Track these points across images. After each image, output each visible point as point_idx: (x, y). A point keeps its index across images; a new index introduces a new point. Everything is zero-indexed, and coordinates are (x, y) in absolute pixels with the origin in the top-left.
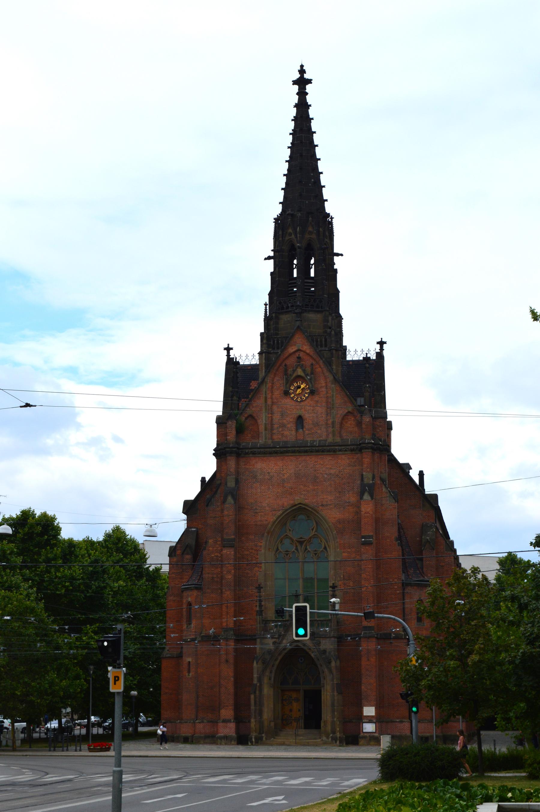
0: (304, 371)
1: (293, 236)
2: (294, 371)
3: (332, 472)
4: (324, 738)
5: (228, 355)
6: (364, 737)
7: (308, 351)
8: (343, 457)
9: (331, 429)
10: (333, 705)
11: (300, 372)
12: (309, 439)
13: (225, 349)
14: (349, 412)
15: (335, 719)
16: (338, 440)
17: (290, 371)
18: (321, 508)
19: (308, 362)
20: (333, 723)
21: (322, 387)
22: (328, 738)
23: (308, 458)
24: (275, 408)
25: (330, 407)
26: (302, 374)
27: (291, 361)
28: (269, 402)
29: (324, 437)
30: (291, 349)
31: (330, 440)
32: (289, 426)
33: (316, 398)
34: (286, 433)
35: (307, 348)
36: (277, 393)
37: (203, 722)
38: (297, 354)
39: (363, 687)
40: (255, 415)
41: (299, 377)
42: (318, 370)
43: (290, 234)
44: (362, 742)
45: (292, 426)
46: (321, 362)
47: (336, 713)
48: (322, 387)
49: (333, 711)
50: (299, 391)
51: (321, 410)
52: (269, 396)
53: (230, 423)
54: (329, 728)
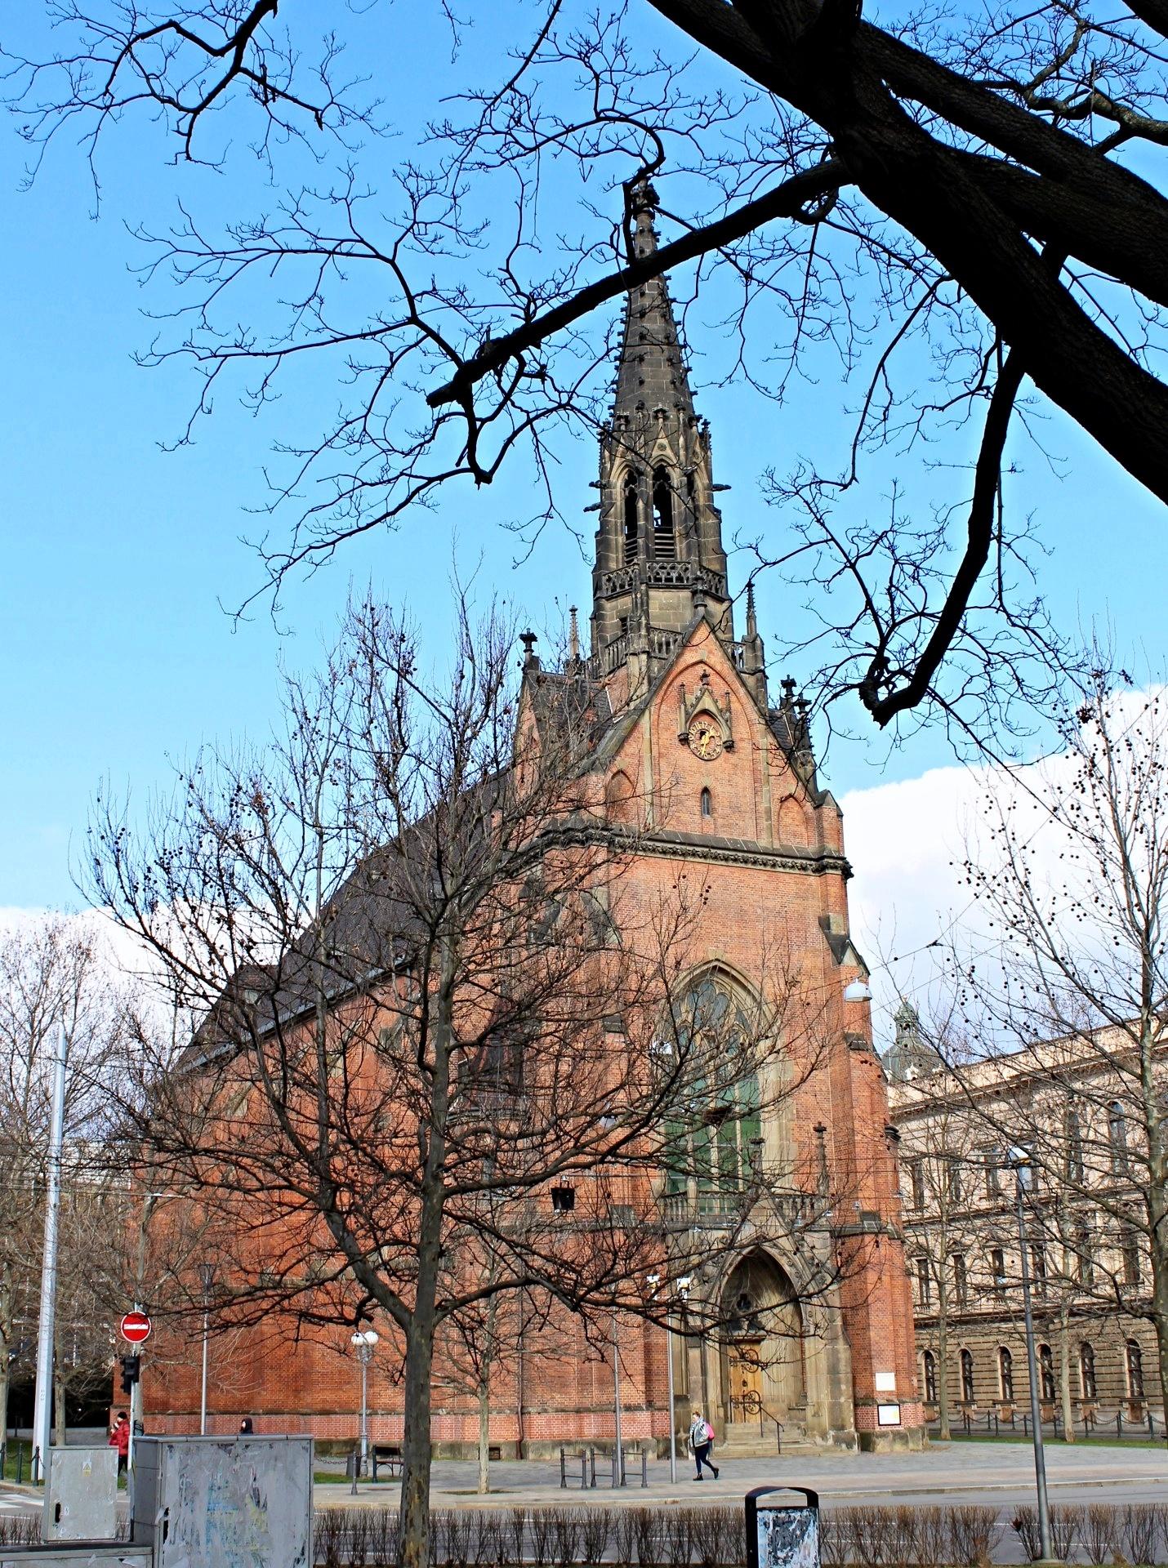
0: (716, 702)
1: (669, 452)
2: (698, 699)
3: (769, 904)
4: (819, 1440)
5: (529, 650)
6: (883, 1435)
7: (718, 668)
8: (786, 877)
9: (764, 823)
10: (833, 1370)
11: (707, 703)
12: (725, 836)
13: (523, 637)
14: (791, 796)
15: (842, 1400)
16: (777, 845)
17: (690, 699)
18: (754, 972)
19: (718, 686)
20: (835, 1407)
21: (742, 740)
22: (824, 1436)
23: (727, 871)
24: (663, 763)
25: (758, 781)
26: (713, 709)
27: (691, 678)
28: (655, 753)
29: (750, 836)
30: (690, 657)
31: (763, 843)
32: (689, 803)
33: (733, 758)
34: (685, 817)
35: (717, 659)
36: (669, 737)
37: (545, 1411)
38: (700, 670)
39: (872, 1334)
40: (629, 772)
41: (705, 712)
42: (735, 706)
43: (662, 448)
44: (881, 1446)
45: (694, 804)
46: (742, 691)
47: (843, 1387)
48: (742, 740)
49: (835, 1382)
50: (705, 739)
51: (744, 781)
52: (654, 740)
53: (594, 778)
54: (825, 1420)
